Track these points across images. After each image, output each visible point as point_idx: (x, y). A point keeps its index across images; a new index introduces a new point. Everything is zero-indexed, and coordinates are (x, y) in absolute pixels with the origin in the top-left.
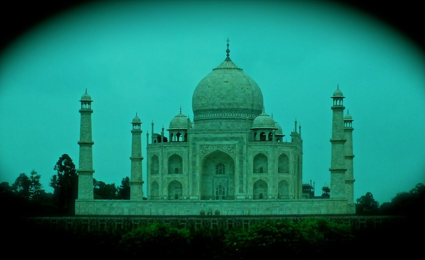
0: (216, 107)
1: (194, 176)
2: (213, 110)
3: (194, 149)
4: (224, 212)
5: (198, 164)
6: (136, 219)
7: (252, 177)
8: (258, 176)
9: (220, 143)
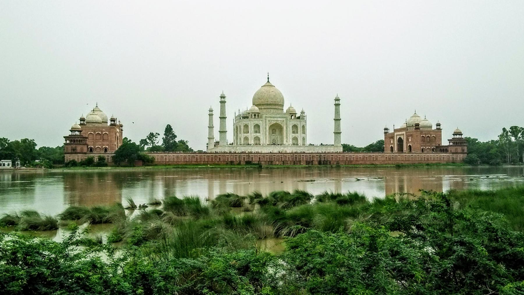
1: (266, 134)
3: (266, 122)
5: (268, 129)
7: (291, 135)
8: (294, 135)
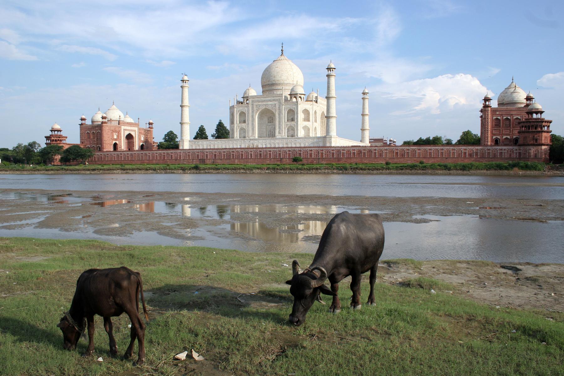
0: (270, 83)
2: (269, 84)
3: (253, 107)
4: (260, 146)
6: (207, 151)
8: (290, 123)
9: (267, 103)
